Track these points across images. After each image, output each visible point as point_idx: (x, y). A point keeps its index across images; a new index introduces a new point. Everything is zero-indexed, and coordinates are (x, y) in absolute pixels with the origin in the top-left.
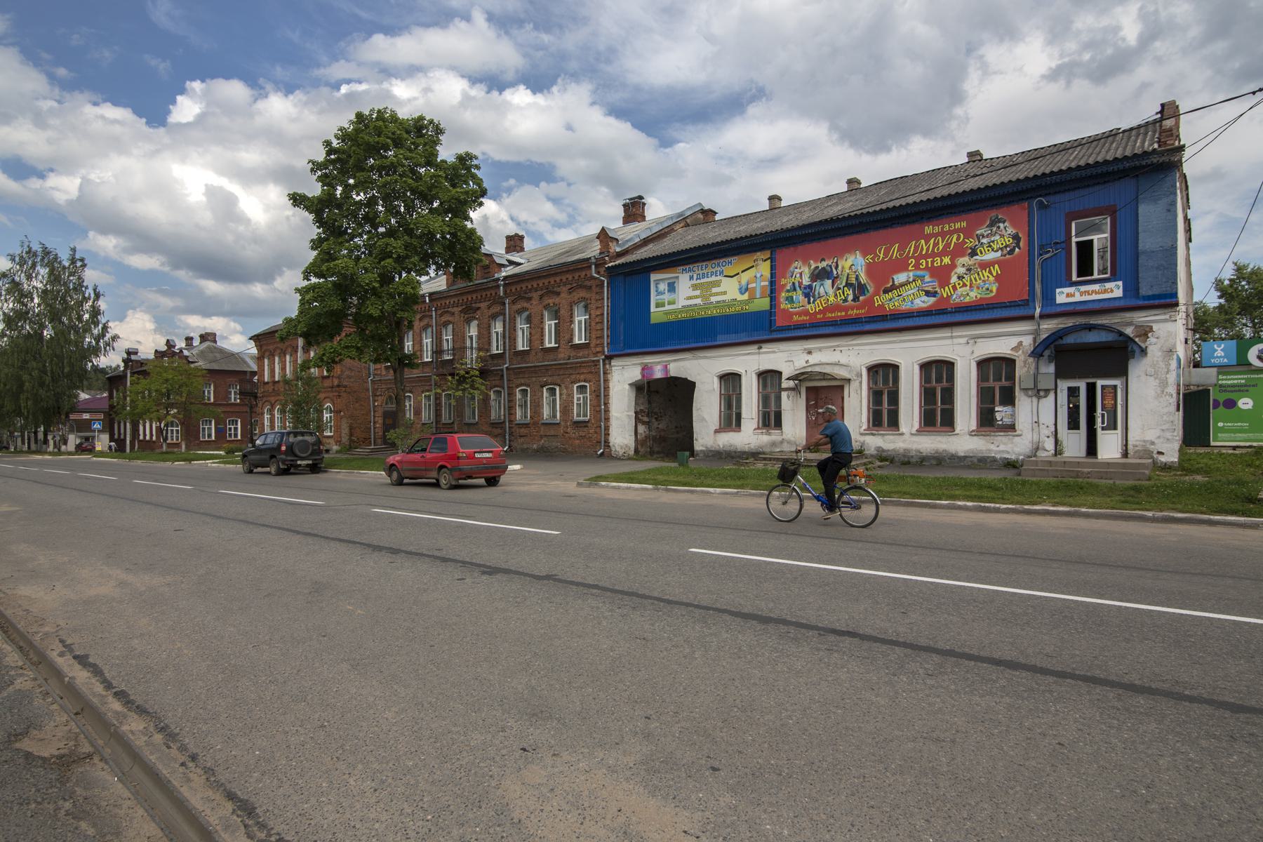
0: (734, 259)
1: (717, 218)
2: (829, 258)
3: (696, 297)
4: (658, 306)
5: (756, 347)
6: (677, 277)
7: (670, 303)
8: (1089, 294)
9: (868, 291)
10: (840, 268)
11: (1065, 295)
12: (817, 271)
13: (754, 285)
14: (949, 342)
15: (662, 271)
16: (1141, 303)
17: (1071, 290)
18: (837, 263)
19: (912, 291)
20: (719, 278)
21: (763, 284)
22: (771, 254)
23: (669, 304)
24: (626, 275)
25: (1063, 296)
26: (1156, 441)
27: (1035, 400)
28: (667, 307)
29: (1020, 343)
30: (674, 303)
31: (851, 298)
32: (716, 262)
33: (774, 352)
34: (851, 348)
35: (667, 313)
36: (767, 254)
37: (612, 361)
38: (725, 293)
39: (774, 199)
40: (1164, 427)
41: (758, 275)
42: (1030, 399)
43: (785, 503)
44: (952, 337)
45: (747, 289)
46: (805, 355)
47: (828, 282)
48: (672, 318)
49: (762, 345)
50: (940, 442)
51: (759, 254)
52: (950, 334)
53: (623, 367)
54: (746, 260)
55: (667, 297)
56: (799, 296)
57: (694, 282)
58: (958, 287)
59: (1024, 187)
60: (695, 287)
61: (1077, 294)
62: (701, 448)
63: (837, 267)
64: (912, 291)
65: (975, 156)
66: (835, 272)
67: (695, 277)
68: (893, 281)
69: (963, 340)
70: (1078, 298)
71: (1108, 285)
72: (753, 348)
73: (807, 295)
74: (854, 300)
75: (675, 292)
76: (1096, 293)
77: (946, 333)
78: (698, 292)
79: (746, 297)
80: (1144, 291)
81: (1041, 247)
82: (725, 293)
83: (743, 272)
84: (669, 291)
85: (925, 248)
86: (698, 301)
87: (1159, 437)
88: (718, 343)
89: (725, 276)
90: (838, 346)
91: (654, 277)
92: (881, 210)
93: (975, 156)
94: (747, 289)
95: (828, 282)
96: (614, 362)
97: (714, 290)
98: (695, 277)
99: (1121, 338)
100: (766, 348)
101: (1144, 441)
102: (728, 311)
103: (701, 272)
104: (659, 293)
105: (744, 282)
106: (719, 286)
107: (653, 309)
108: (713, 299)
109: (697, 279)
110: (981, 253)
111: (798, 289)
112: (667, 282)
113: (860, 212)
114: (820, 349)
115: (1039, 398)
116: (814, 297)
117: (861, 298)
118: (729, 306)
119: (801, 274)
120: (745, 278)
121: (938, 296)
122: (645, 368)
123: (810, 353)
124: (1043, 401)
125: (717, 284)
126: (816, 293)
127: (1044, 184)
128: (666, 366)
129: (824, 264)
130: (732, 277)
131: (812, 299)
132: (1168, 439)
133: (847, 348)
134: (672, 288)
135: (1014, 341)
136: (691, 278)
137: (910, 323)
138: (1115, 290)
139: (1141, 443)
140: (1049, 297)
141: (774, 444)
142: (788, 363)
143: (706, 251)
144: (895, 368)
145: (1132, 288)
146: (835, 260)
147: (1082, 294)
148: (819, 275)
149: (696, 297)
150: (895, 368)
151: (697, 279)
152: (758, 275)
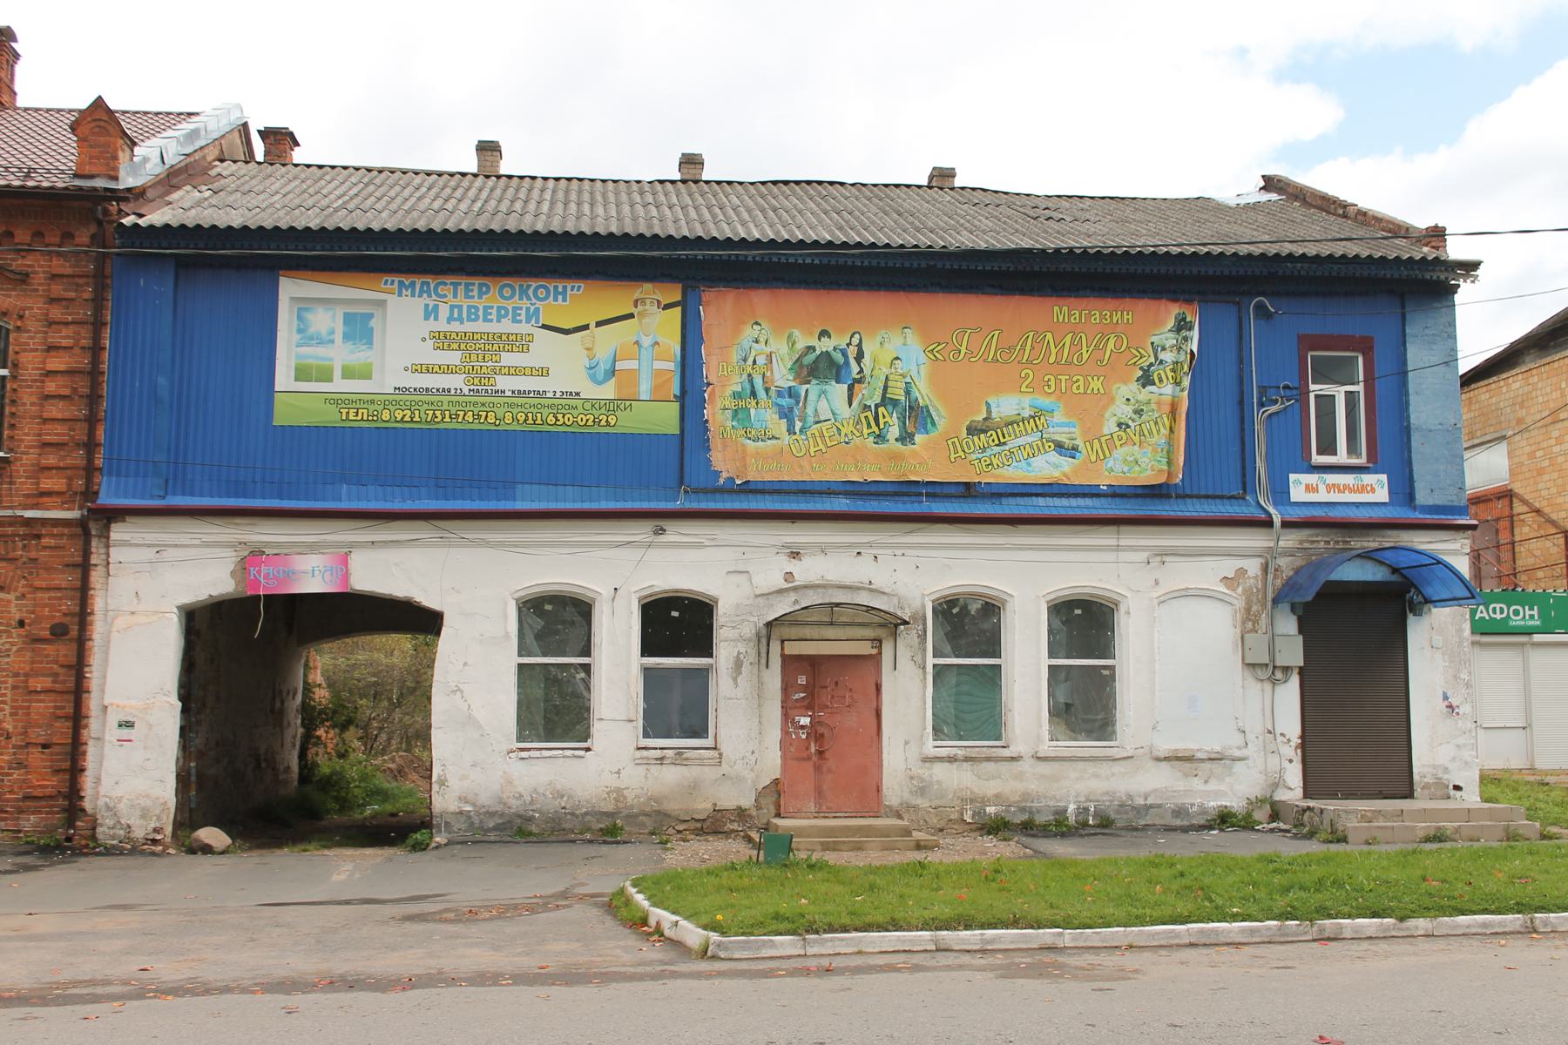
0: (576, 289)
1: (298, 156)
2: (841, 331)
3: (448, 370)
4: (302, 374)
5: (648, 526)
6: (382, 304)
7: (348, 374)
8: (1340, 491)
9: (933, 423)
10: (867, 361)
11: (1303, 487)
12: (811, 357)
13: (633, 365)
14: (1111, 556)
16: (1418, 516)
17: (1312, 478)
18: (860, 345)
19: (1029, 439)
20: (524, 328)
21: (658, 365)
22: (684, 294)
23: (344, 377)
24: (184, 266)
25: (1304, 488)
26: (1450, 766)
27: (1268, 686)
28: (339, 385)
29: (1241, 572)
30: (366, 375)
31: (894, 432)
32: (516, 283)
33: (699, 546)
34: (899, 552)
35: (336, 400)
36: (674, 293)
37: (114, 527)
38: (543, 372)
39: (691, 162)
40: (1461, 741)
41: (646, 342)
42: (1259, 685)
43: (1206, 782)
44: (1118, 548)
45: (612, 372)
46: (783, 559)
47: (839, 391)
48: (357, 418)
49: (665, 524)
50: (1096, 776)
51: (648, 286)
52: (1113, 542)
53: (160, 548)
54: (615, 300)
55: (340, 354)
56: (766, 416)
57: (442, 325)
58: (1118, 443)
59: (1203, 270)
60: (443, 341)
61: (1322, 488)
62: (453, 806)
63: (859, 357)
64: (1029, 439)
65: (942, 177)
66: (855, 368)
67: (444, 311)
68: (989, 411)
69: (1143, 556)
70: (1322, 496)
71: (1368, 479)
72: (640, 531)
73: (786, 414)
74: (901, 439)
75: (370, 343)
76: (1352, 490)
77: (1104, 538)
78: (453, 358)
79: (608, 391)
80: (1422, 497)
81: (1263, 390)
82: (543, 372)
83: (599, 324)
84: (347, 337)
85: (1054, 351)
86: (456, 382)
87: (1454, 759)
88: (520, 505)
89: (544, 327)
90: (870, 545)
91: (290, 289)
92: (1250, 255)
93: (942, 177)
94: (612, 372)
95: (839, 391)
96: (118, 532)
97: (508, 359)
98: (444, 311)
99: (1394, 578)
100: (678, 532)
101: (1434, 767)
102: (548, 421)
103: (465, 304)
104: (307, 337)
105: (603, 354)
106: (524, 349)
107: (284, 379)
108: (505, 383)
109: (450, 320)
110: (1161, 381)
111: (761, 394)
112: (340, 313)
113: (1206, 250)
114: (823, 550)
115: (1274, 682)
116: (803, 419)
117: (918, 438)
118: (556, 410)
119: (769, 357)
120: (607, 341)
121: (1080, 457)
122: (253, 557)
123: (795, 555)
124: (1280, 689)
125: (520, 343)
126: (810, 411)
127: (1280, 273)
128: (344, 560)
129: (826, 345)
130: (566, 332)
131: (798, 425)
132: (1466, 763)
133: (890, 551)
134: (359, 328)
135: (1229, 567)
136: (430, 313)
137: (1042, 506)
138: (1376, 489)
139: (1431, 770)
140: (1281, 493)
141: (694, 787)
142: (735, 578)
143: (700, 254)
144: (992, 608)
145: (1404, 490)
146: (856, 340)
147: (1329, 488)
148: (821, 368)
149: (448, 370)
150: (992, 608)
151: (450, 320)
152: (646, 342)
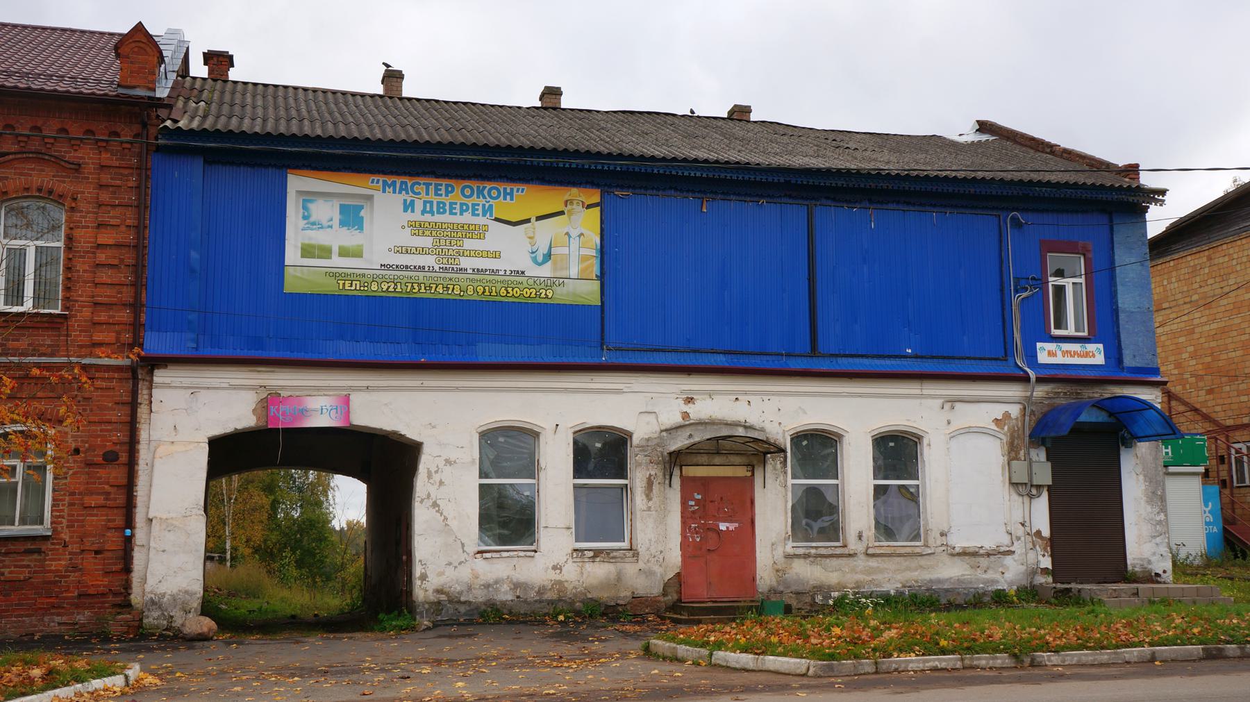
3: (422, 251)
6: (370, 198)
7: (344, 253)
8: (1071, 356)
11: (1046, 352)
13: (565, 251)
15: (298, 171)
17: (1051, 346)
20: (481, 220)
23: (341, 255)
25: (1046, 353)
27: (1026, 499)
28: (337, 261)
29: (1007, 415)
30: (357, 253)
32: (475, 184)
33: (619, 392)
34: (766, 398)
38: (496, 255)
41: (574, 233)
42: (1021, 499)
44: (922, 396)
45: (548, 256)
48: (351, 288)
51: (574, 191)
52: (918, 392)
53: (194, 390)
54: (549, 198)
55: (338, 237)
57: (417, 216)
60: (418, 228)
61: (1059, 353)
67: (419, 205)
70: (1060, 360)
71: (1091, 347)
75: (361, 228)
76: (1079, 356)
78: (426, 242)
79: (546, 271)
80: (1128, 361)
81: (1017, 280)
82: (496, 255)
83: (539, 218)
86: (429, 261)
87: (1154, 554)
89: (497, 220)
90: (746, 393)
91: (296, 183)
93: (740, 113)
96: (160, 376)
97: (469, 244)
98: (419, 205)
101: (1141, 559)
102: (501, 294)
103: (435, 200)
107: (292, 255)
108: (466, 263)
109: (424, 212)
114: (710, 394)
115: (1031, 497)
120: (546, 232)
122: (270, 400)
124: (1035, 502)
125: (479, 233)
128: (346, 401)
134: (351, 217)
136: (409, 206)
138: (1095, 355)
140: (1031, 356)
145: (1115, 353)
147: (1065, 353)
149: (422, 251)
152: (574, 233)
